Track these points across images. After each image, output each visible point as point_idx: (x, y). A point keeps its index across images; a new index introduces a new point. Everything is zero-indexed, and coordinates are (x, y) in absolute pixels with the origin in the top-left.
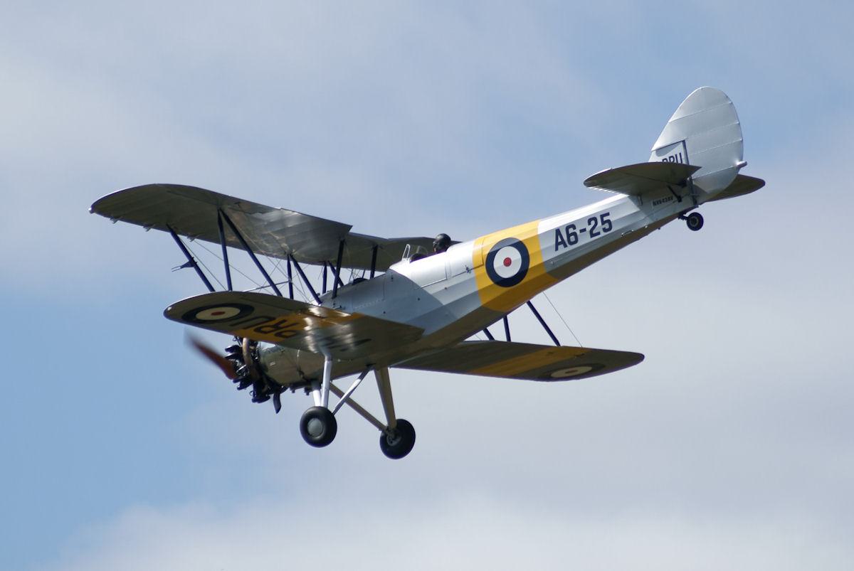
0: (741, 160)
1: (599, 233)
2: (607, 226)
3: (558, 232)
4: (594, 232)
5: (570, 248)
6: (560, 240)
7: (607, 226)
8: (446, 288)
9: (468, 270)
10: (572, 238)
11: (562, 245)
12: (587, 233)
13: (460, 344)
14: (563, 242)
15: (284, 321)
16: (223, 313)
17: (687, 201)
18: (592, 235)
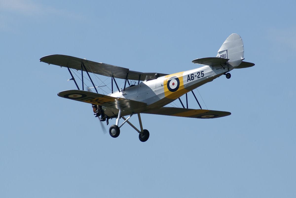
0: (243, 58)
1: (200, 77)
2: (202, 75)
3: (188, 76)
4: (199, 77)
5: (192, 81)
6: (189, 78)
7: (202, 75)
8: (155, 91)
9: (162, 85)
10: (192, 78)
11: (189, 80)
12: (197, 77)
13: (162, 108)
14: (190, 79)
15: (98, 99)
16: (77, 96)
17: (226, 70)
18: (198, 78)
